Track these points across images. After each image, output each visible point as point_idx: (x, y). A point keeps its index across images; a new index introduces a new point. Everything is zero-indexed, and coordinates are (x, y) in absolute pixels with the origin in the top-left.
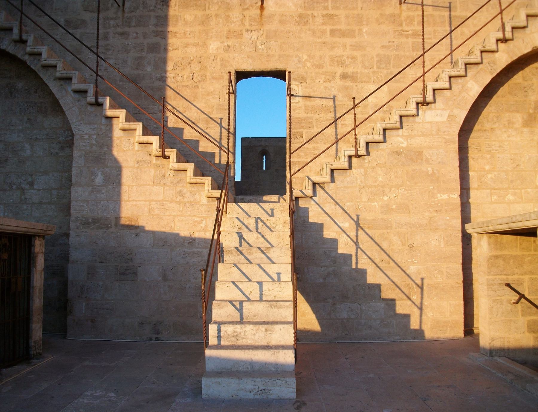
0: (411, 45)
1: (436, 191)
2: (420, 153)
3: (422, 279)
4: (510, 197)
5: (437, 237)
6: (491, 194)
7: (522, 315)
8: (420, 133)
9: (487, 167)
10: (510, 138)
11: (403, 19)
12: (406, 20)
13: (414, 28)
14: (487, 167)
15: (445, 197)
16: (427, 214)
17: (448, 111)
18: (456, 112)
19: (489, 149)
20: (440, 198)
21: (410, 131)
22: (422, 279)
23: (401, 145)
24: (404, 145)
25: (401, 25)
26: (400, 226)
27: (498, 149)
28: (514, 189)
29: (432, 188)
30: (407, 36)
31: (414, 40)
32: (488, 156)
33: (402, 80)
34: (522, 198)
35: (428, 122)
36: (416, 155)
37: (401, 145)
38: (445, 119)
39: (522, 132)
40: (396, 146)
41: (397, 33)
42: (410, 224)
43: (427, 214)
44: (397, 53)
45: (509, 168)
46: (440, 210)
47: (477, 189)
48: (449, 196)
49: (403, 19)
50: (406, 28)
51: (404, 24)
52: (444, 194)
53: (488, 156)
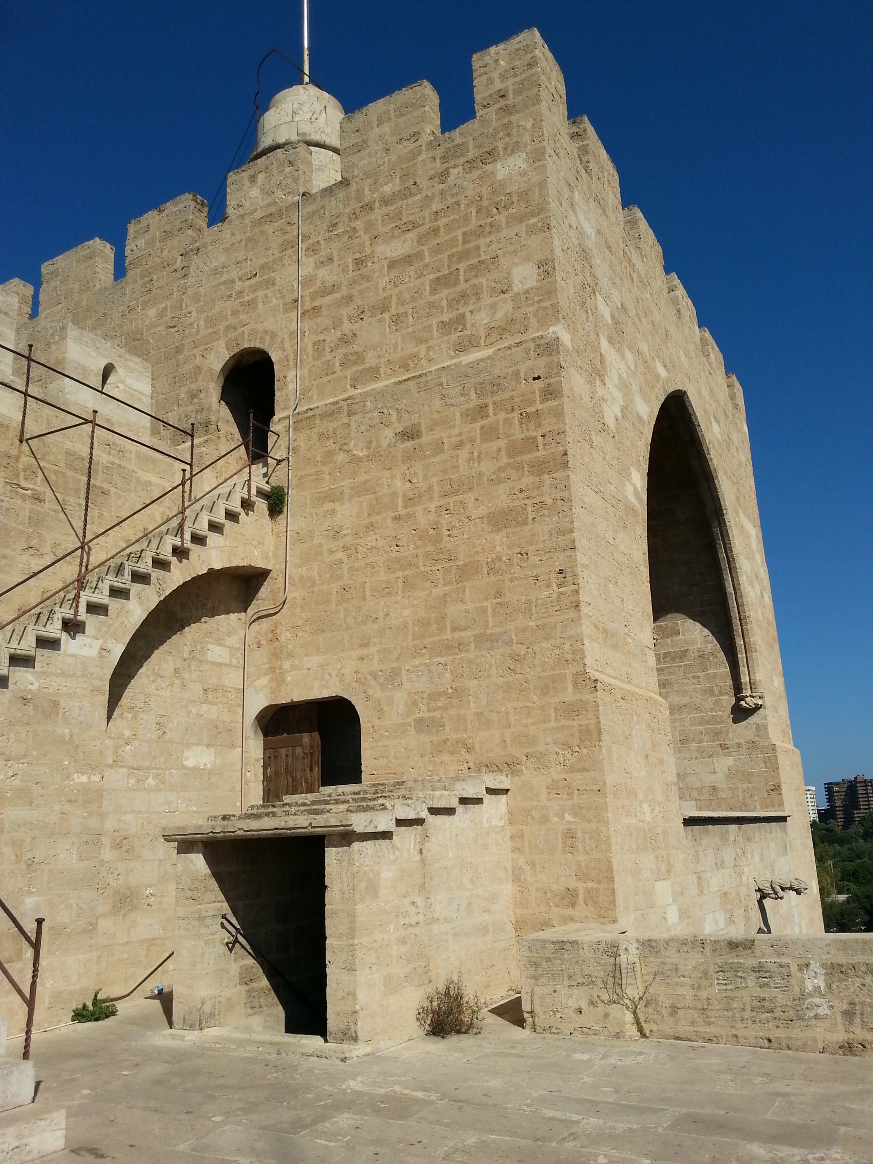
0: (27, 514)
1: (72, 770)
2: (55, 704)
3: (40, 922)
4: (151, 782)
5: (67, 847)
6: (129, 775)
7: (235, 960)
8: (59, 671)
9: (127, 733)
10: (158, 692)
11: (21, 466)
12: (24, 470)
13: (36, 488)
14: (127, 733)
15: (84, 779)
16: (57, 807)
17: (101, 641)
18: (110, 645)
19: (132, 705)
20: (77, 781)
21: (45, 665)
22: (40, 922)
23: (30, 687)
24: (35, 687)
25: (18, 475)
26: (16, 828)
27: (142, 706)
28: (157, 769)
29: (66, 763)
30: (24, 498)
31: (33, 507)
32: (130, 716)
33: (7, 569)
34: (164, 783)
35: (72, 655)
36: (51, 708)
37: (30, 687)
38: (94, 652)
39: (172, 685)
40: (22, 687)
41: (9, 488)
42: (32, 824)
43: (57, 807)
44: (5, 521)
45: (153, 737)
46: (76, 801)
47: (111, 766)
48: (89, 778)
49: (21, 466)
50: (24, 484)
51: (21, 477)
52: (82, 774)
53: (130, 716)
